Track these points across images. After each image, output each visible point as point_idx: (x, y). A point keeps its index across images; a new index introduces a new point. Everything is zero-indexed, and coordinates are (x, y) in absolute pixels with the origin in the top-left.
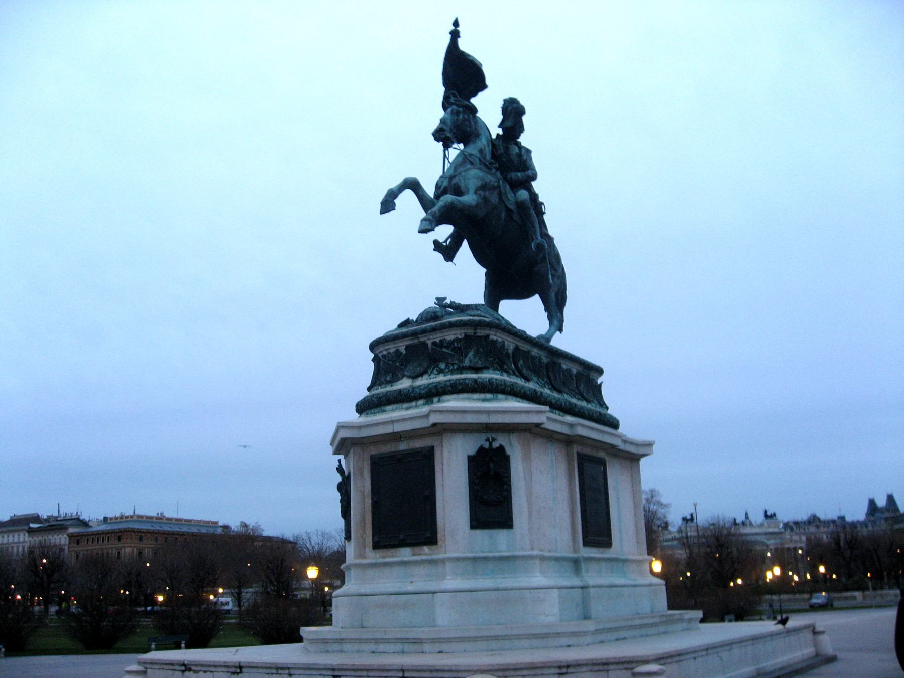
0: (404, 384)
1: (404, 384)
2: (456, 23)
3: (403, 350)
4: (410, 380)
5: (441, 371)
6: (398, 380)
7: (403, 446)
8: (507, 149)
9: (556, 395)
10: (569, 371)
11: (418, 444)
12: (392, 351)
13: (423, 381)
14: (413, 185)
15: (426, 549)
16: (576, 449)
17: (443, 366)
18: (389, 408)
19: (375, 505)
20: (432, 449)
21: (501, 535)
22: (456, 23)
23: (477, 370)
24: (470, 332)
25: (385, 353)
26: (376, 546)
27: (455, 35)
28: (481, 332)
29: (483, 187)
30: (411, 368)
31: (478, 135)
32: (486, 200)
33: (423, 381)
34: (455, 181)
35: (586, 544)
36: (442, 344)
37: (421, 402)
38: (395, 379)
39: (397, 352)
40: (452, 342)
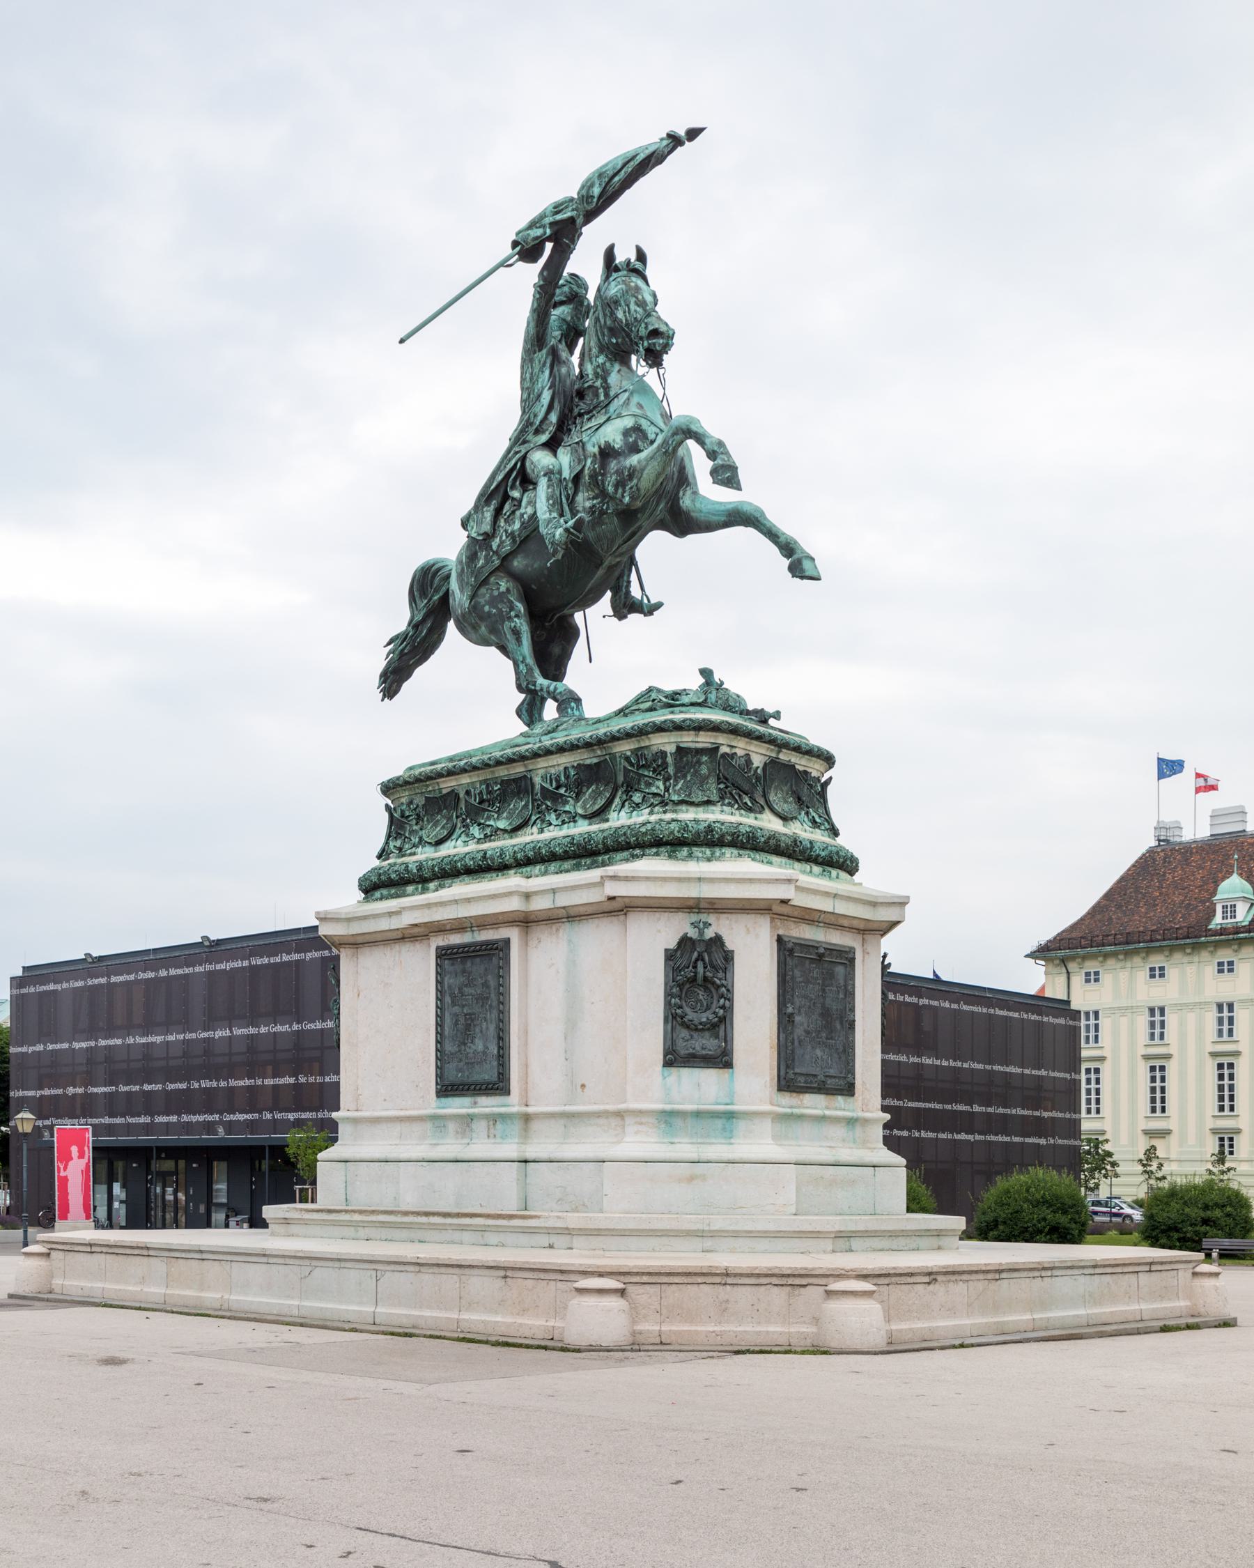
2: (693, 134)
4: (781, 822)
12: (740, 753)
22: (693, 134)
25: (727, 750)
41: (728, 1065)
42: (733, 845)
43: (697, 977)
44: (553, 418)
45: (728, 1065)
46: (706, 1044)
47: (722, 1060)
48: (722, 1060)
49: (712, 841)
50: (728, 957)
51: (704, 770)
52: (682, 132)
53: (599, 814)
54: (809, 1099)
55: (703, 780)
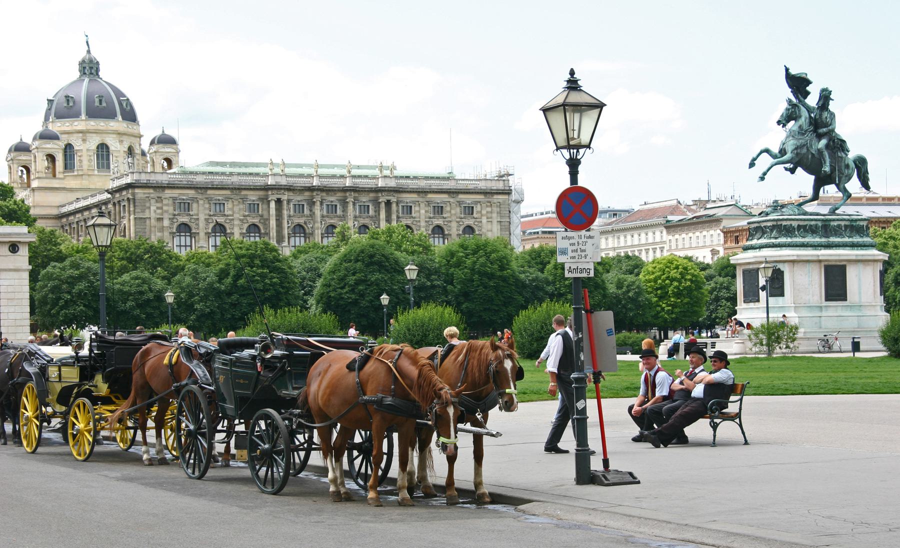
0: (754, 242)
1: (754, 242)
7: (751, 267)
8: (821, 115)
9: (823, 240)
10: (839, 226)
11: (755, 266)
14: (767, 151)
16: (823, 264)
21: (781, 298)
23: (776, 238)
24: (775, 223)
27: (787, 70)
28: (779, 223)
29: (796, 149)
30: (758, 235)
31: (800, 117)
32: (797, 154)
35: (827, 299)
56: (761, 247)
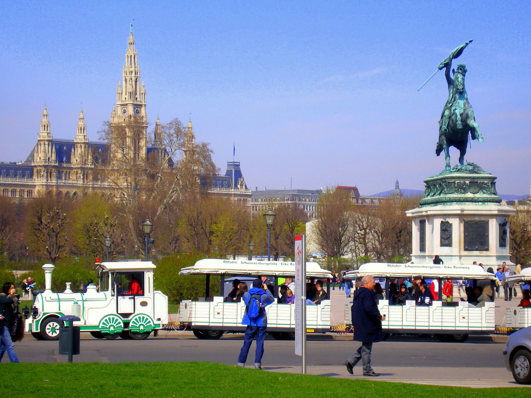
0: (469, 195)
1: (469, 195)
2: (471, 42)
3: (467, 182)
5: (484, 193)
6: (467, 193)
7: (477, 219)
13: (477, 195)
15: (484, 252)
17: (485, 191)
18: (467, 203)
19: (465, 236)
20: (489, 221)
22: (471, 42)
26: (466, 250)
27: (467, 44)
30: (472, 190)
33: (477, 195)
34: (466, 112)
36: (483, 183)
37: (480, 203)
38: (465, 192)
39: (465, 183)
40: (487, 183)
41: (451, 246)
42: (456, 201)
43: (446, 229)
44: (453, 100)
45: (451, 246)
46: (446, 242)
47: (450, 245)
48: (450, 245)
49: (451, 201)
50: (451, 225)
51: (453, 186)
52: (468, 42)
53: (440, 194)
54: (475, 252)
55: (452, 188)
56: (484, 201)
